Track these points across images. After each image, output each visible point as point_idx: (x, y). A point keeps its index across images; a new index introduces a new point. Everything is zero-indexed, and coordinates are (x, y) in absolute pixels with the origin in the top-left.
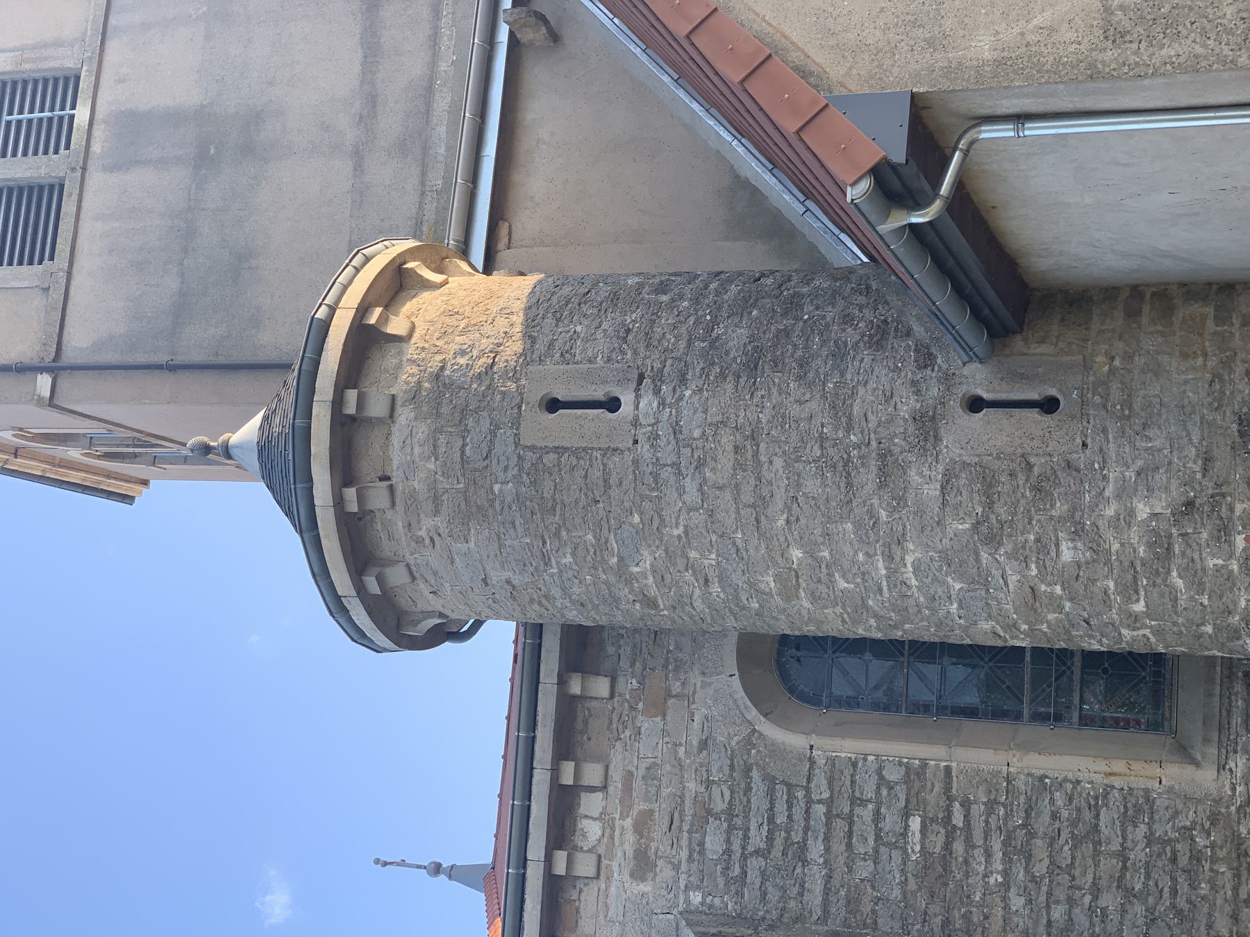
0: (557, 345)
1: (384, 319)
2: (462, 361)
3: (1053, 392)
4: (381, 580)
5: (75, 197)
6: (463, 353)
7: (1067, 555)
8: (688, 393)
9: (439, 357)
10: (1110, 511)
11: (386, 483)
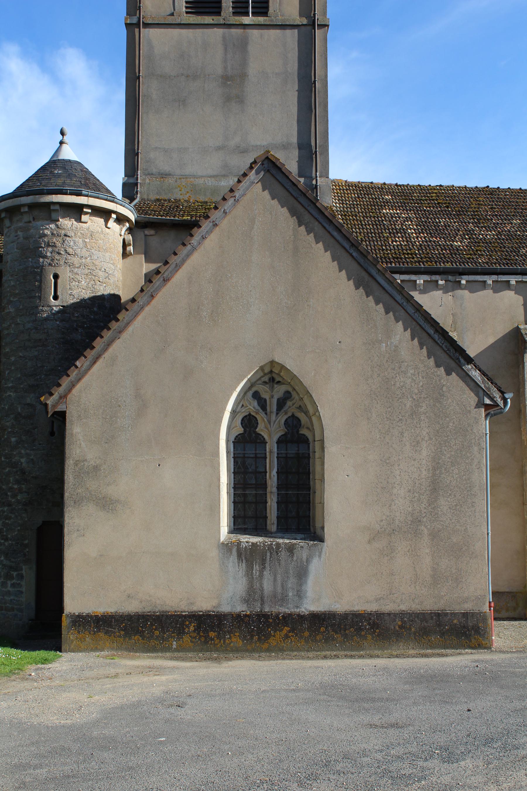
0: (77, 276)
1: (87, 213)
2: (72, 243)
3: (56, 435)
4: (5, 217)
5: (212, 22)
6: (75, 243)
7: (13, 439)
8: (58, 323)
9: (73, 235)
10: (23, 452)
11: (32, 220)
